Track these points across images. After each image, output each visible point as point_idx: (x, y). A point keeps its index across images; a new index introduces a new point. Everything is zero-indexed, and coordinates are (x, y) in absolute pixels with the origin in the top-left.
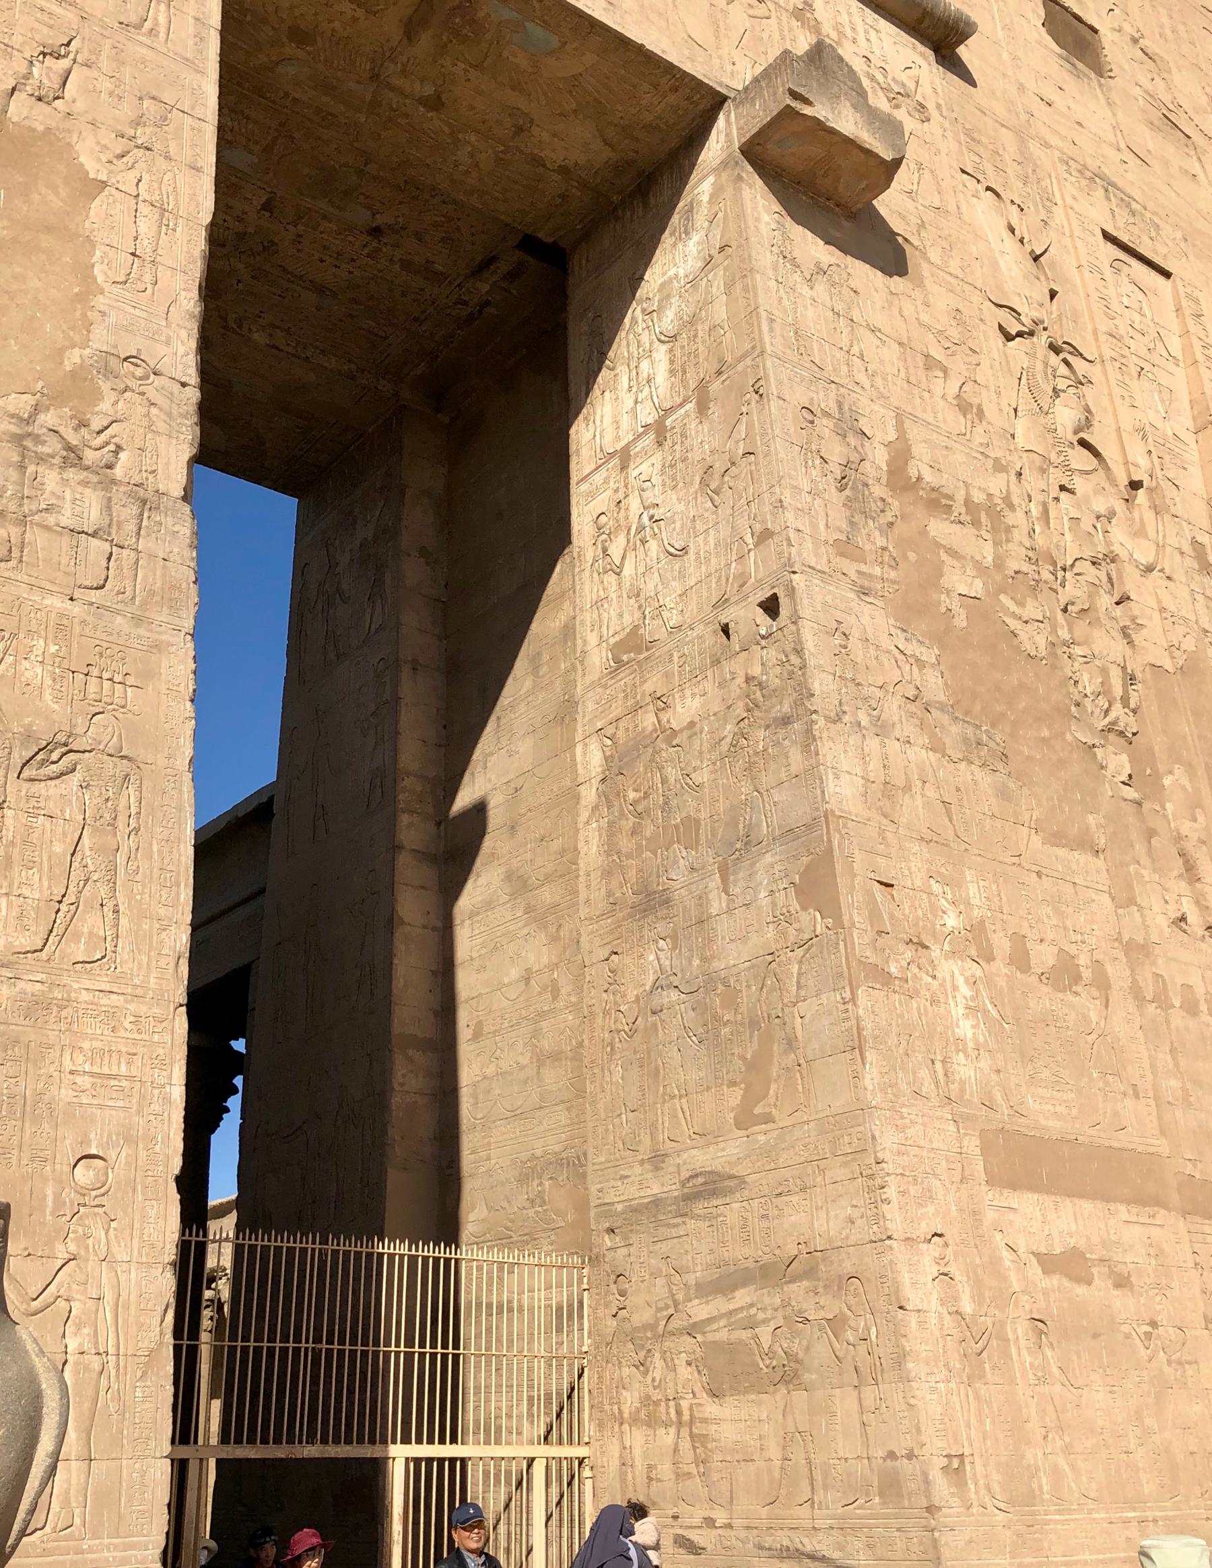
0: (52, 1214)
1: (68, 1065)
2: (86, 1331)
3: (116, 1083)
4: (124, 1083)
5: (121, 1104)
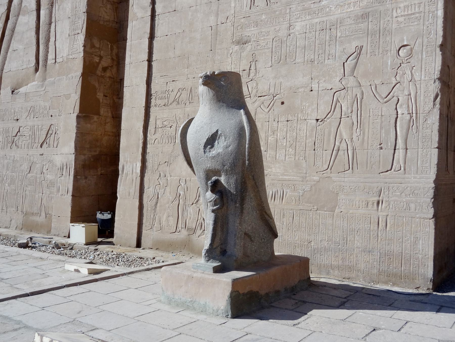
1: (395, 14)
2: (404, 106)
3: (414, 16)
4: (417, 15)
5: (416, 23)
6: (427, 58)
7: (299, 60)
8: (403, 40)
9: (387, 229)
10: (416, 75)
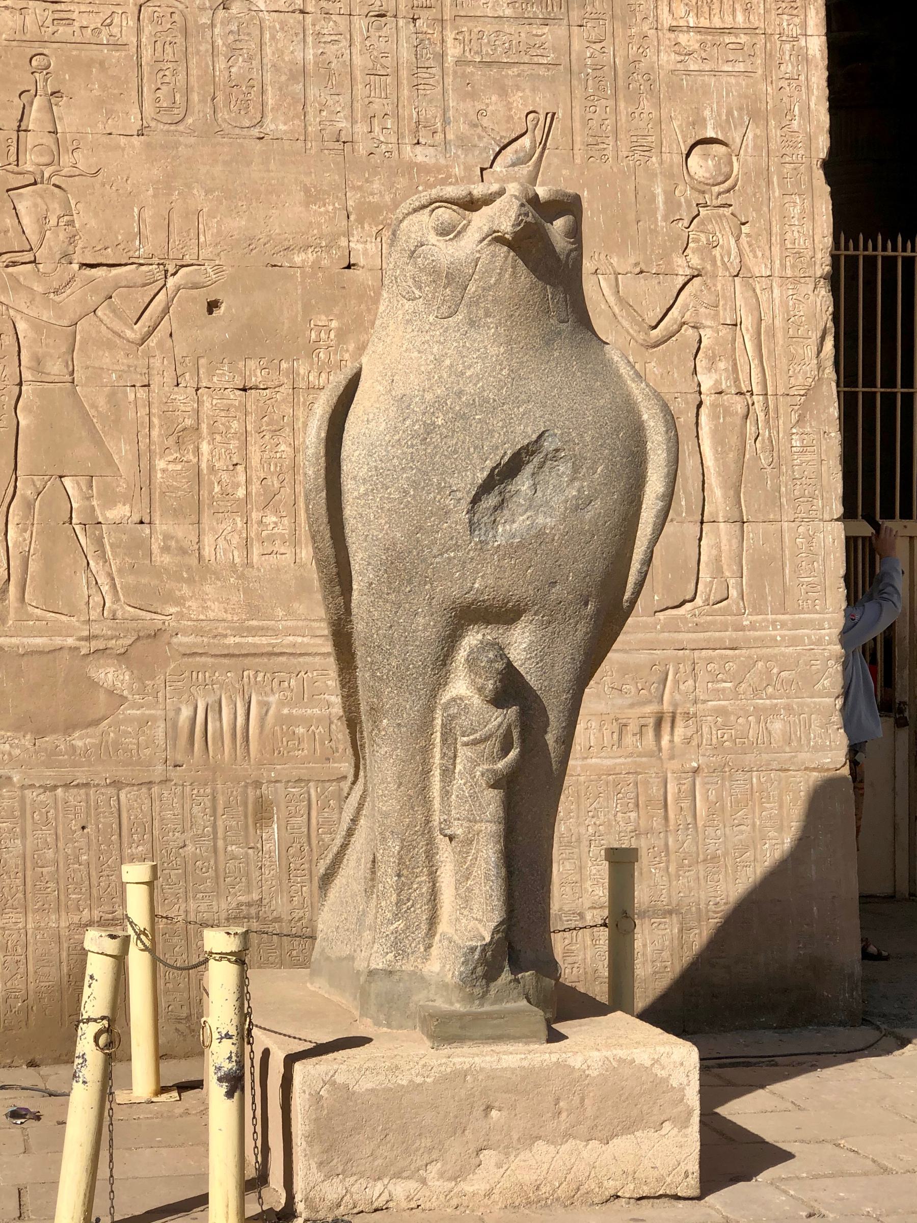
0: (665, 218)
1: (666, 20)
2: (722, 365)
3: (733, 39)
4: (743, 39)
5: (741, 67)
6: (787, 199)
7: (282, 127)
8: (700, 122)
9: (700, 823)
10: (755, 256)
